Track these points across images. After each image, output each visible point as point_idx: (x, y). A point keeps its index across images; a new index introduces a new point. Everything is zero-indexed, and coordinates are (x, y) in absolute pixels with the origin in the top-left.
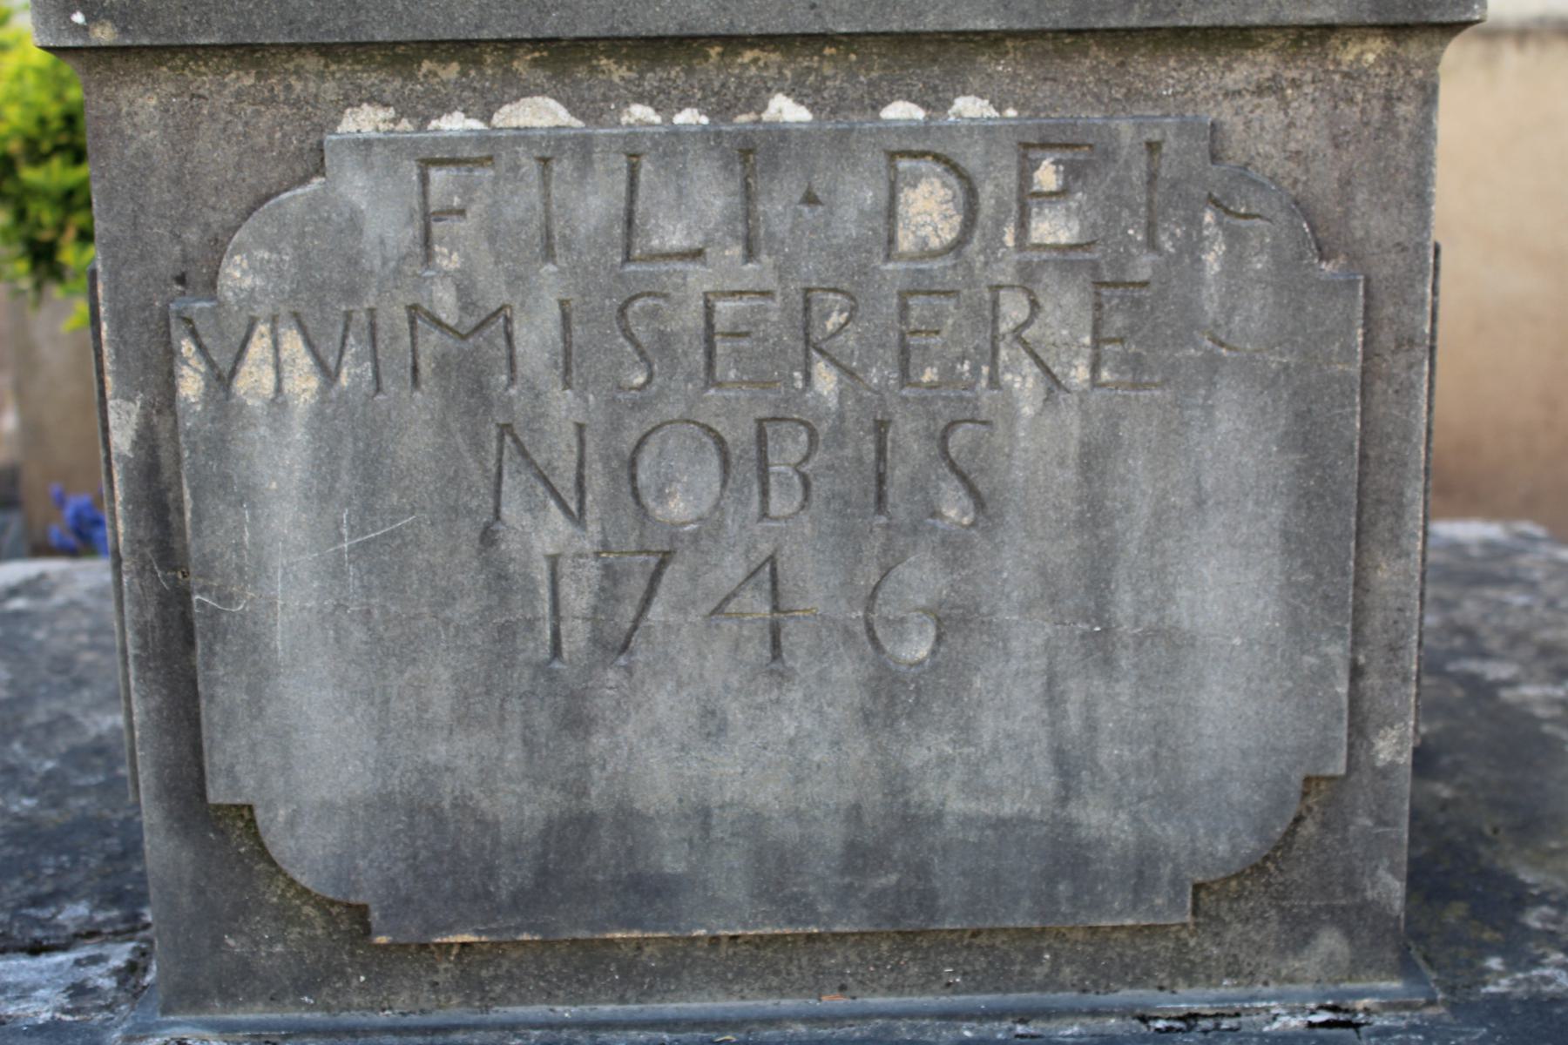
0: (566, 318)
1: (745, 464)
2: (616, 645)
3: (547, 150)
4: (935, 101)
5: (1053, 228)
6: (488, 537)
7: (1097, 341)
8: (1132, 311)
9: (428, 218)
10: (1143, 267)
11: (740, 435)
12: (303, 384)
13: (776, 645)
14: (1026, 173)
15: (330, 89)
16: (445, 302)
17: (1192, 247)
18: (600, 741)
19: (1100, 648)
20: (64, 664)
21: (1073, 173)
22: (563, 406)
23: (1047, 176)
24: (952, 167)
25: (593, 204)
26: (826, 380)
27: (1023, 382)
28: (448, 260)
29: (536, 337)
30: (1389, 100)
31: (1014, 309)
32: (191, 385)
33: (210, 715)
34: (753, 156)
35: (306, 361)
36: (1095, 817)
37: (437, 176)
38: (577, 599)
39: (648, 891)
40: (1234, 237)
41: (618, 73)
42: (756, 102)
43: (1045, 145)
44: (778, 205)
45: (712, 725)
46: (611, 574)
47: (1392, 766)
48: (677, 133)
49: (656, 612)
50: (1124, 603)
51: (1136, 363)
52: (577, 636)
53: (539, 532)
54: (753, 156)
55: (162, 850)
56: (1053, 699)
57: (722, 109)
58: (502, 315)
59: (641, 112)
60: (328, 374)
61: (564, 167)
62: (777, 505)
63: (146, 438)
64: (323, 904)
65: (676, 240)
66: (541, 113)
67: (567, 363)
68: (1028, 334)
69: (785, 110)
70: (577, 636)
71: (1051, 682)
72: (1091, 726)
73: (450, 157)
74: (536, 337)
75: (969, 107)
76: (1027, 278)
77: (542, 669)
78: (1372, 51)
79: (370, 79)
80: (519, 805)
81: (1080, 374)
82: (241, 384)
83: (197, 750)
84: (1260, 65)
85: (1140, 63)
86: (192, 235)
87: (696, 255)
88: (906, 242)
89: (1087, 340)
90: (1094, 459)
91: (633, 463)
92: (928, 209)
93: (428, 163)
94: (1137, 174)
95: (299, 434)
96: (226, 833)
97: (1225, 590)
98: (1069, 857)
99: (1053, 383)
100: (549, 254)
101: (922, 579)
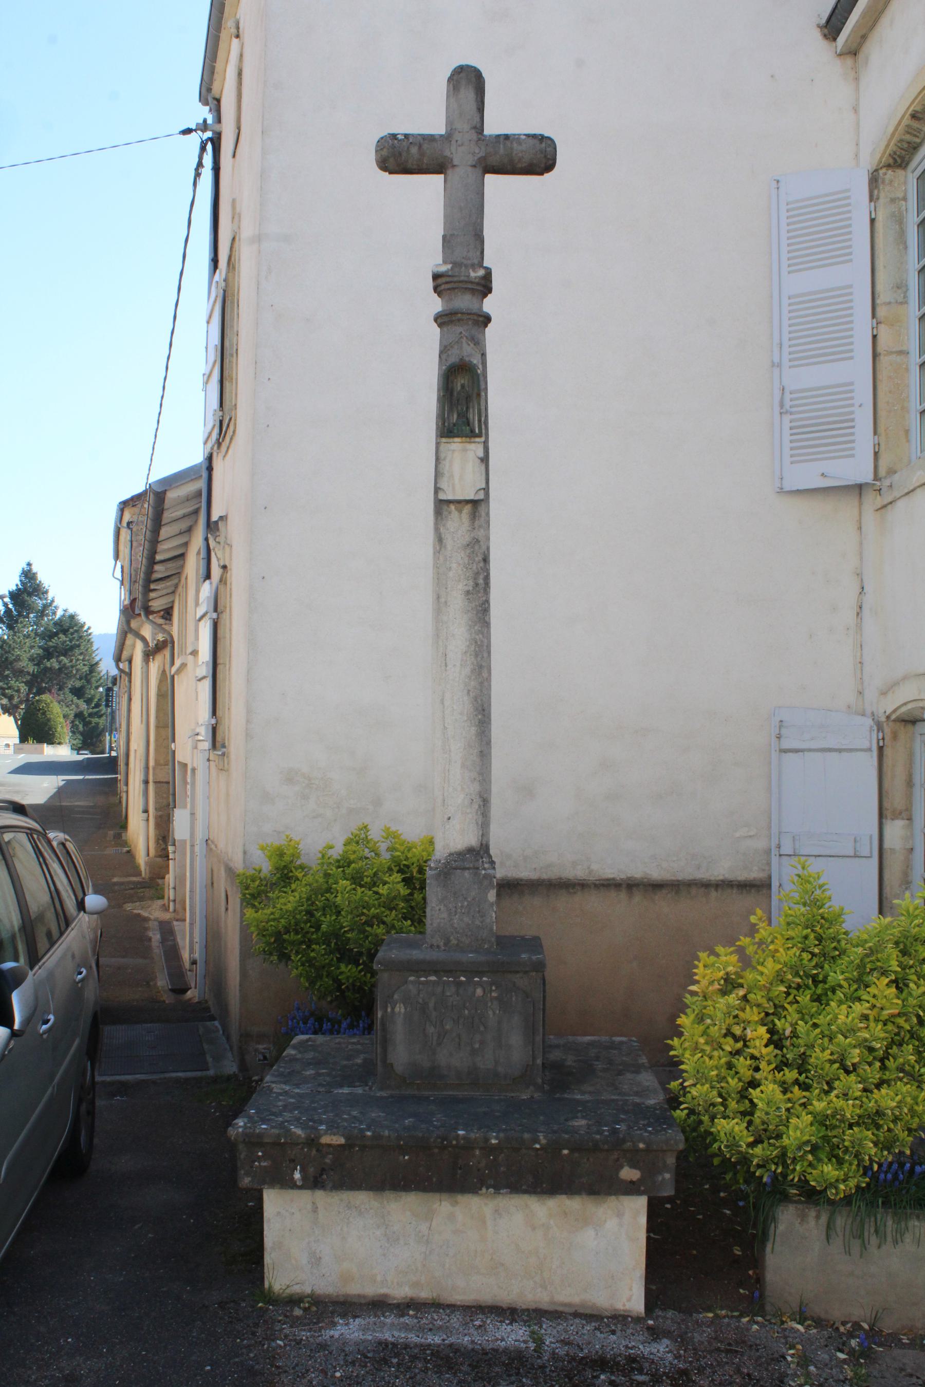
2: (439, 1044)
4: (481, 978)
5: (494, 994)
9: (419, 991)
12: (403, 1010)
16: (421, 1001)
21: (497, 988)
22: (434, 1014)
23: (494, 988)
25: (439, 989)
26: (466, 1012)
27: (490, 1013)
28: (421, 996)
29: (431, 1005)
31: (489, 1004)
32: (389, 1010)
36: (500, 1069)
38: (435, 1038)
53: (431, 1030)
55: (380, 1068)
60: (406, 1009)
65: (448, 994)
66: (433, 978)
67: (435, 1009)
69: (463, 979)
70: (434, 1043)
74: (431, 1005)
75: (485, 979)
78: (534, 973)
92: (479, 992)
96: (389, 1067)
97: (516, 1040)
99: (494, 1013)
101: (478, 1037)
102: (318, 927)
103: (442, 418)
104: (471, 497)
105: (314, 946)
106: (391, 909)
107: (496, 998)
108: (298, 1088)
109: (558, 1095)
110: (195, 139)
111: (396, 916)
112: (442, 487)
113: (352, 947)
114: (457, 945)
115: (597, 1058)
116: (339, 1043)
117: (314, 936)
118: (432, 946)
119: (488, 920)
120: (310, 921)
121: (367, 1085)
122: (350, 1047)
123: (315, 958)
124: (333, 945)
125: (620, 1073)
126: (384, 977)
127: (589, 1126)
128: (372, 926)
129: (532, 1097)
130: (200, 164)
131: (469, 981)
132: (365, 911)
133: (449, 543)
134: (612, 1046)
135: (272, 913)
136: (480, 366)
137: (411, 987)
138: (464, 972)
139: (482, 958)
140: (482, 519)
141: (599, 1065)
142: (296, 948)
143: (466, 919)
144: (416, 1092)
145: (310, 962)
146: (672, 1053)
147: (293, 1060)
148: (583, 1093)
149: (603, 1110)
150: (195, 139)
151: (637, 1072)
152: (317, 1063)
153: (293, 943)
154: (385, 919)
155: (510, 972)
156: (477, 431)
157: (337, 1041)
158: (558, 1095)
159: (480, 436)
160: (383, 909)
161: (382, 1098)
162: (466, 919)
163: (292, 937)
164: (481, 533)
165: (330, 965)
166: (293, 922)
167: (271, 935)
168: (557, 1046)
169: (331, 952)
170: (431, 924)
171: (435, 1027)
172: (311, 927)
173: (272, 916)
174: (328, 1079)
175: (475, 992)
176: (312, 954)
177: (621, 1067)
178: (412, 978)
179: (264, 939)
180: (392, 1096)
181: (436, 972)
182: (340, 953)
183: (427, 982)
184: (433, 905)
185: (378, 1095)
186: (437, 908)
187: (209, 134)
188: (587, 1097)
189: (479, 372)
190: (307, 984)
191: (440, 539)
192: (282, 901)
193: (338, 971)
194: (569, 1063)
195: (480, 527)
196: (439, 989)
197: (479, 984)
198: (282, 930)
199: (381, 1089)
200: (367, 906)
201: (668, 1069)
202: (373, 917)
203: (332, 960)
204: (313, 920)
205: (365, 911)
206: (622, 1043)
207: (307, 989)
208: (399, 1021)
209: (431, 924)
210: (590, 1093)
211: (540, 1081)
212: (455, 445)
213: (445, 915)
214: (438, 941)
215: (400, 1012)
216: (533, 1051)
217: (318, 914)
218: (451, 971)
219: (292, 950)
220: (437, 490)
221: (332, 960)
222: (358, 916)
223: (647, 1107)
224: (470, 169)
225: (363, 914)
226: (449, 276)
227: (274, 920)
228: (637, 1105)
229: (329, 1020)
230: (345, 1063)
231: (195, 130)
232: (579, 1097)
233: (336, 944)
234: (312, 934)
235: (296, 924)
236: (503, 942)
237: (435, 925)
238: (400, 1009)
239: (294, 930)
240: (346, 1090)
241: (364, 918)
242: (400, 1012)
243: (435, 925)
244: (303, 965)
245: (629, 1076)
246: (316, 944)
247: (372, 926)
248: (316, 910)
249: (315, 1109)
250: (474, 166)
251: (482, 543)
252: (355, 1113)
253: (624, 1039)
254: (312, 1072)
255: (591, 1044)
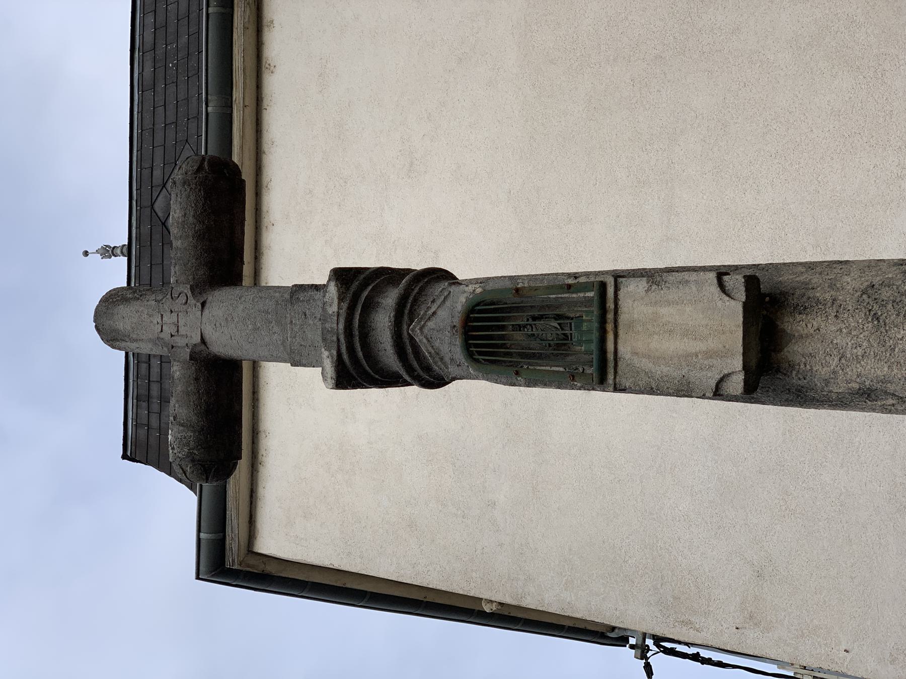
103: (570, 379)
104: (732, 312)
110: (658, 660)
112: (713, 383)
130: (696, 657)
133: (872, 370)
136: (470, 288)
140: (816, 280)
150: (658, 660)
156: (591, 294)
159: (603, 286)
164: (852, 282)
187: (649, 642)
189: (479, 290)
191: (865, 397)
195: (832, 286)
212: (633, 347)
220: (718, 394)
224: (206, 311)
226: (339, 355)
231: (647, 659)
250: (203, 304)
251: (877, 280)
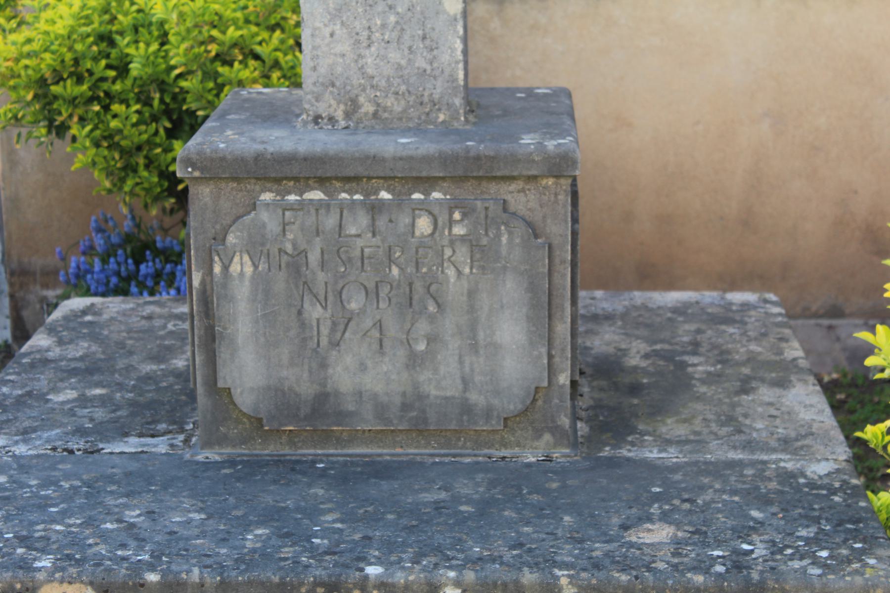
0: (322, 252)
1: (373, 293)
2: (335, 344)
3: (319, 206)
4: (427, 193)
5: (459, 230)
6: (300, 313)
7: (472, 261)
8: (482, 254)
9: (284, 225)
10: (484, 241)
11: (371, 285)
12: (249, 269)
13: (381, 345)
14: (451, 214)
15: (257, 188)
16: (289, 247)
17: (498, 236)
18: (330, 371)
19: (474, 348)
20: (121, 345)
21: (464, 215)
22: (321, 276)
23: (457, 216)
24: (430, 213)
25: (330, 221)
26: (395, 271)
27: (451, 272)
28: (290, 236)
29: (314, 257)
30: (556, 195)
31: (448, 252)
32: (217, 269)
33: (219, 362)
34: (375, 209)
35: (249, 263)
37: (287, 213)
38: (325, 331)
39: (342, 416)
40: (510, 233)
41: (338, 185)
42: (376, 193)
43: (456, 207)
44: (382, 222)
45: (363, 367)
46: (334, 324)
47: (564, 385)
48: (353, 201)
49: (347, 335)
50: (481, 335)
51: (483, 268)
52: (324, 341)
53: (314, 312)
54: (375, 209)
55: (202, 399)
56: (461, 362)
57: (367, 195)
58: (305, 252)
59: (344, 195)
60: (256, 267)
61: (322, 211)
62: (381, 305)
63: (203, 283)
64: (249, 417)
65: (353, 231)
66: (316, 195)
67: (323, 265)
68: (453, 259)
69: (385, 195)
70: (324, 341)
71: (460, 357)
72: (472, 370)
73: (291, 207)
74: (314, 257)
75: (436, 195)
76: (452, 243)
77: (315, 351)
78: (551, 181)
79: (269, 185)
80: (307, 389)
81: (467, 270)
82: (231, 269)
83: (215, 372)
84: (520, 184)
85: (484, 184)
86: (218, 227)
87: (359, 236)
88: (417, 233)
89: (469, 261)
90: (472, 294)
91: (341, 293)
92: (424, 225)
93: (284, 210)
94: (482, 216)
95: (247, 283)
96: (222, 396)
98: (467, 409)
99: (459, 273)
100: (318, 234)
101: (423, 327)
102: (122, 69)
105: (116, 107)
106: (272, 29)
107: (462, 239)
108: (25, 441)
109: (607, 452)
111: (282, 42)
113: (194, 106)
114: (375, 115)
115: (695, 347)
116: (150, 318)
117: (118, 87)
118: (317, 119)
119: (445, 58)
120: (108, 56)
121: (182, 430)
122: (170, 326)
123: (120, 131)
124: (156, 103)
125: (745, 389)
126: (202, 196)
127: (677, 542)
128: (230, 64)
129: (548, 459)
131: (400, 202)
132: (215, 33)
134: (727, 316)
135: (29, 41)
137: (264, 216)
138: (388, 180)
139: (428, 148)
141: (699, 366)
142: (80, 111)
143: (394, 56)
144: (287, 451)
145: (109, 140)
146: (870, 362)
147: (42, 362)
148: (665, 443)
149: (708, 496)
151: (782, 384)
152: (87, 370)
153: (72, 101)
154: (258, 49)
155: (495, 178)
157: (149, 310)
158: (607, 452)
160: (254, 29)
161: (207, 465)
162: (394, 56)
163: (70, 88)
165: (151, 144)
166: (69, 57)
167: (27, 87)
168: (609, 317)
169: (155, 118)
170: (314, 69)
171: (325, 308)
172: (109, 67)
173: (27, 49)
174: (100, 414)
175: (413, 225)
176: (114, 124)
177: (746, 371)
178: (267, 197)
179: (13, 96)
180: (231, 462)
181: (322, 182)
182: (170, 120)
183: (301, 206)
184: (317, 24)
185: (200, 458)
186: (327, 31)
188: (673, 456)
190: (107, 184)
192: (49, 14)
193: (170, 156)
194: (634, 361)
196: (330, 221)
197: (425, 207)
198: (48, 75)
199: (207, 444)
200: (219, 22)
201: (826, 322)
202: (235, 45)
203: (156, 133)
204: (114, 53)
205: (215, 33)
206: (746, 307)
207: (110, 191)
208: (242, 291)
209: (314, 69)
210: (680, 442)
211: (565, 421)
213: (344, 47)
214: (330, 105)
215: (242, 274)
216: (550, 357)
217: (123, 42)
218: (356, 179)
219: (71, 116)
221: (156, 133)
222: (202, 43)
223: (812, 485)
225: (212, 39)
227: (29, 55)
228: (787, 477)
229: (157, 253)
230: (149, 368)
232: (653, 454)
233: (162, 101)
234: (114, 82)
235: (76, 61)
236: (483, 104)
237: (322, 70)
238: (242, 266)
239: (71, 75)
240: (132, 445)
241: (214, 49)
242: (242, 274)
243: (322, 70)
244: (97, 145)
245: (766, 393)
246: (122, 102)
247: (230, 64)
248: (121, 33)
249: (43, 505)
252: (132, 515)
253: (750, 297)
254: (71, 394)
255: (681, 310)
